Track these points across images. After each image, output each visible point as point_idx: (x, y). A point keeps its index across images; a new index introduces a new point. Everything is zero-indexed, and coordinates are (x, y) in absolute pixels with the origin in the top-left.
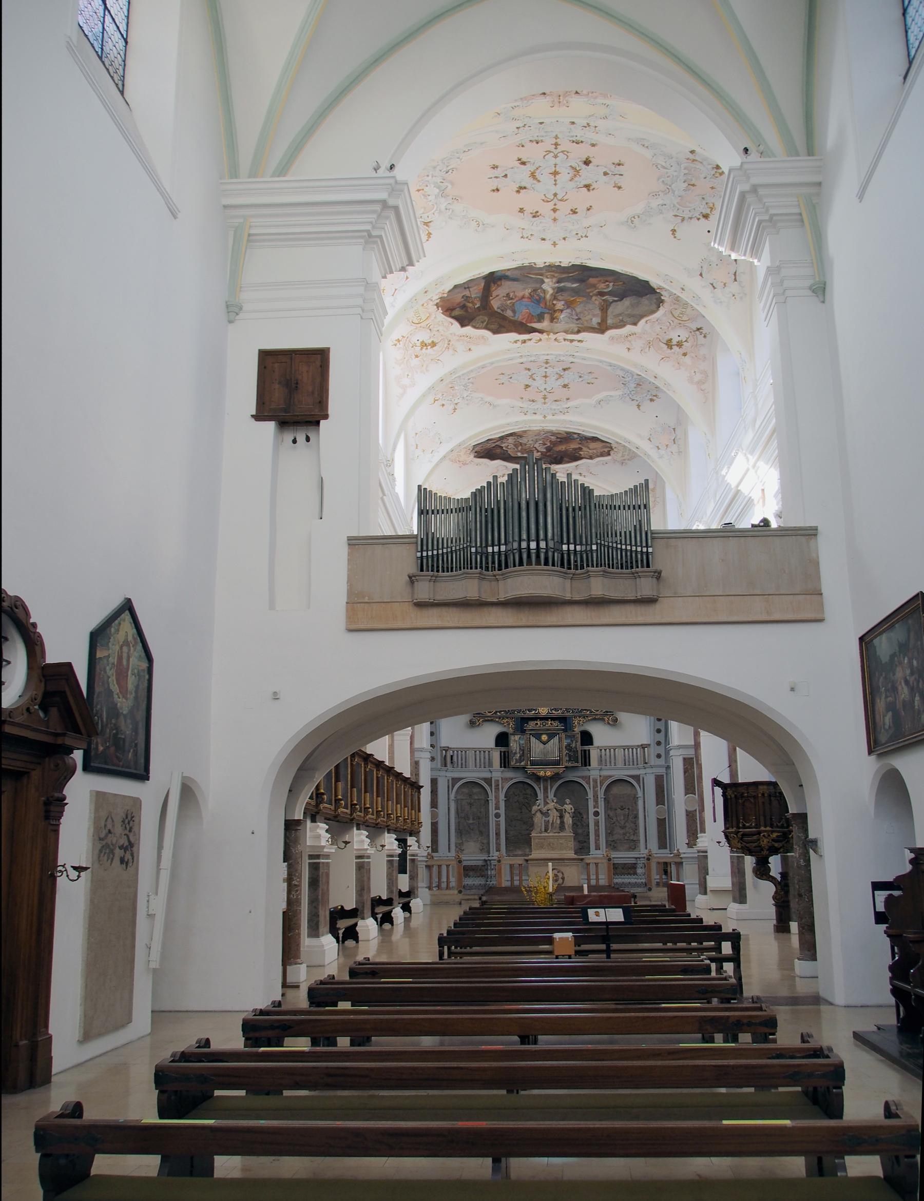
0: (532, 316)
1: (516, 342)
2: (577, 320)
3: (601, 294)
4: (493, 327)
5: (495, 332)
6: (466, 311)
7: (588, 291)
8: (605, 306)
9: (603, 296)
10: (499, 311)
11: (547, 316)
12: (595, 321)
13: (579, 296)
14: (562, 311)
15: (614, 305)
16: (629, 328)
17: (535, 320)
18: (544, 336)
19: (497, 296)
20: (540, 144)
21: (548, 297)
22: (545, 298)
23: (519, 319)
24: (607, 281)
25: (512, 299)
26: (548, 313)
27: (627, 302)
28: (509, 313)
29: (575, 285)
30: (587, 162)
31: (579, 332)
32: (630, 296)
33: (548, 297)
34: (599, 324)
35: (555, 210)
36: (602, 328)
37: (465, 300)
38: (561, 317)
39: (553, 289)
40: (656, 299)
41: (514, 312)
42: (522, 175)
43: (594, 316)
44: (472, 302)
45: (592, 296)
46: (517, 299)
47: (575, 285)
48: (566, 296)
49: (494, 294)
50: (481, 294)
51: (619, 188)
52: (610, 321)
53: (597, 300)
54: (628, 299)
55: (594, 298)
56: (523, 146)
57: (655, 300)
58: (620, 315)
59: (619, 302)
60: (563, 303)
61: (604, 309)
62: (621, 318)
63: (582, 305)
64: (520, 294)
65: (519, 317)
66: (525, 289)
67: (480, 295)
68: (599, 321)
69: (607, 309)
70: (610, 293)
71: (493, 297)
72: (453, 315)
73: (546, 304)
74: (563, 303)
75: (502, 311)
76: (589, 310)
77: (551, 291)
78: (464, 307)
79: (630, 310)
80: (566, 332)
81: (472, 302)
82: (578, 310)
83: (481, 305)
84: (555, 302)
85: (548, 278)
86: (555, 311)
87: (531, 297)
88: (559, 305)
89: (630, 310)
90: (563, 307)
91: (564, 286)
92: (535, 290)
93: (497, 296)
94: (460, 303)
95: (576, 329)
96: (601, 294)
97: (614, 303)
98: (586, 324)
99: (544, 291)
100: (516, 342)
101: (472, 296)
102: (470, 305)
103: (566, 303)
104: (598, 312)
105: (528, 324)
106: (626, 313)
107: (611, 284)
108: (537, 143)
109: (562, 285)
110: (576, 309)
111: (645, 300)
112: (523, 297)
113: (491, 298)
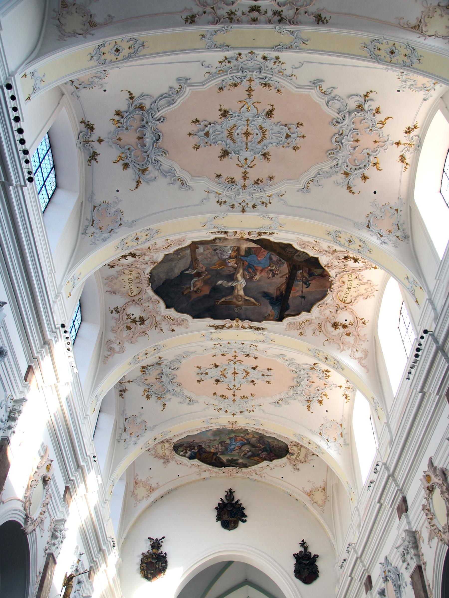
0: (255, 254)
1: (271, 234)
2: (217, 249)
3: (198, 275)
4: (291, 250)
5: (290, 246)
6: (310, 270)
7: (209, 276)
8: (194, 263)
9: (197, 272)
10: (283, 261)
11: (243, 253)
12: (201, 250)
13: (216, 270)
14: (230, 257)
15: (188, 266)
16: (171, 251)
17: (253, 250)
18: (246, 236)
19: (282, 277)
20: (243, 395)
21: (241, 271)
22: (244, 270)
23: (267, 252)
24: (196, 292)
25: (271, 270)
26: (242, 256)
27: (177, 272)
28: (275, 258)
29: (220, 282)
30: (217, 381)
31: (215, 239)
32: (176, 278)
33: (241, 271)
34: (197, 248)
35: (234, 395)
36: (194, 245)
37: (308, 281)
38: (230, 252)
39: (237, 280)
40: (155, 281)
41: (271, 259)
42: (253, 375)
43: (202, 254)
44: (303, 276)
45: (206, 270)
46: (267, 270)
47: (220, 282)
48: (227, 271)
49: (284, 280)
50: (295, 283)
51: (198, 367)
52: (188, 252)
53: (201, 267)
54: (176, 275)
55: (204, 269)
56: (252, 394)
57: (155, 279)
58: (180, 259)
59: (183, 269)
60: (229, 264)
61: (194, 261)
62: (179, 256)
63: (213, 262)
64: (264, 274)
65: (266, 254)
66: (260, 280)
67: (296, 283)
68: (197, 250)
69: (192, 261)
70: (191, 277)
71: (285, 276)
72: (322, 270)
73: (243, 264)
74: (229, 264)
75: (280, 260)
76: (207, 258)
77: (239, 276)
78: (311, 274)
79: (173, 264)
80: (225, 239)
81: (303, 276)
82: (216, 258)
83: (297, 271)
84: (236, 265)
85: (241, 296)
86: (236, 257)
87: (255, 271)
88: (232, 262)
89: (173, 264)
90: (229, 261)
91: (229, 281)
92: (252, 278)
93: (282, 277)
94: (313, 280)
95: (217, 241)
96: (198, 275)
97: (187, 268)
98: (209, 246)
99: (244, 276)
100: (271, 234)
101: (301, 283)
102: (306, 275)
103: (227, 264)
104: (199, 258)
105: (259, 246)
106: (176, 262)
107: (192, 289)
108: (244, 396)
109: (230, 284)
110: (218, 259)
111: (163, 277)
112: (262, 271)
113: (287, 276)
